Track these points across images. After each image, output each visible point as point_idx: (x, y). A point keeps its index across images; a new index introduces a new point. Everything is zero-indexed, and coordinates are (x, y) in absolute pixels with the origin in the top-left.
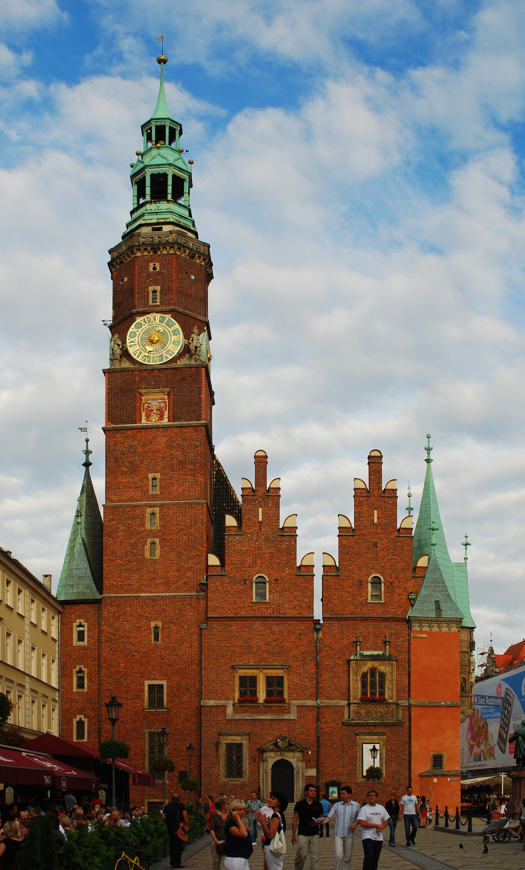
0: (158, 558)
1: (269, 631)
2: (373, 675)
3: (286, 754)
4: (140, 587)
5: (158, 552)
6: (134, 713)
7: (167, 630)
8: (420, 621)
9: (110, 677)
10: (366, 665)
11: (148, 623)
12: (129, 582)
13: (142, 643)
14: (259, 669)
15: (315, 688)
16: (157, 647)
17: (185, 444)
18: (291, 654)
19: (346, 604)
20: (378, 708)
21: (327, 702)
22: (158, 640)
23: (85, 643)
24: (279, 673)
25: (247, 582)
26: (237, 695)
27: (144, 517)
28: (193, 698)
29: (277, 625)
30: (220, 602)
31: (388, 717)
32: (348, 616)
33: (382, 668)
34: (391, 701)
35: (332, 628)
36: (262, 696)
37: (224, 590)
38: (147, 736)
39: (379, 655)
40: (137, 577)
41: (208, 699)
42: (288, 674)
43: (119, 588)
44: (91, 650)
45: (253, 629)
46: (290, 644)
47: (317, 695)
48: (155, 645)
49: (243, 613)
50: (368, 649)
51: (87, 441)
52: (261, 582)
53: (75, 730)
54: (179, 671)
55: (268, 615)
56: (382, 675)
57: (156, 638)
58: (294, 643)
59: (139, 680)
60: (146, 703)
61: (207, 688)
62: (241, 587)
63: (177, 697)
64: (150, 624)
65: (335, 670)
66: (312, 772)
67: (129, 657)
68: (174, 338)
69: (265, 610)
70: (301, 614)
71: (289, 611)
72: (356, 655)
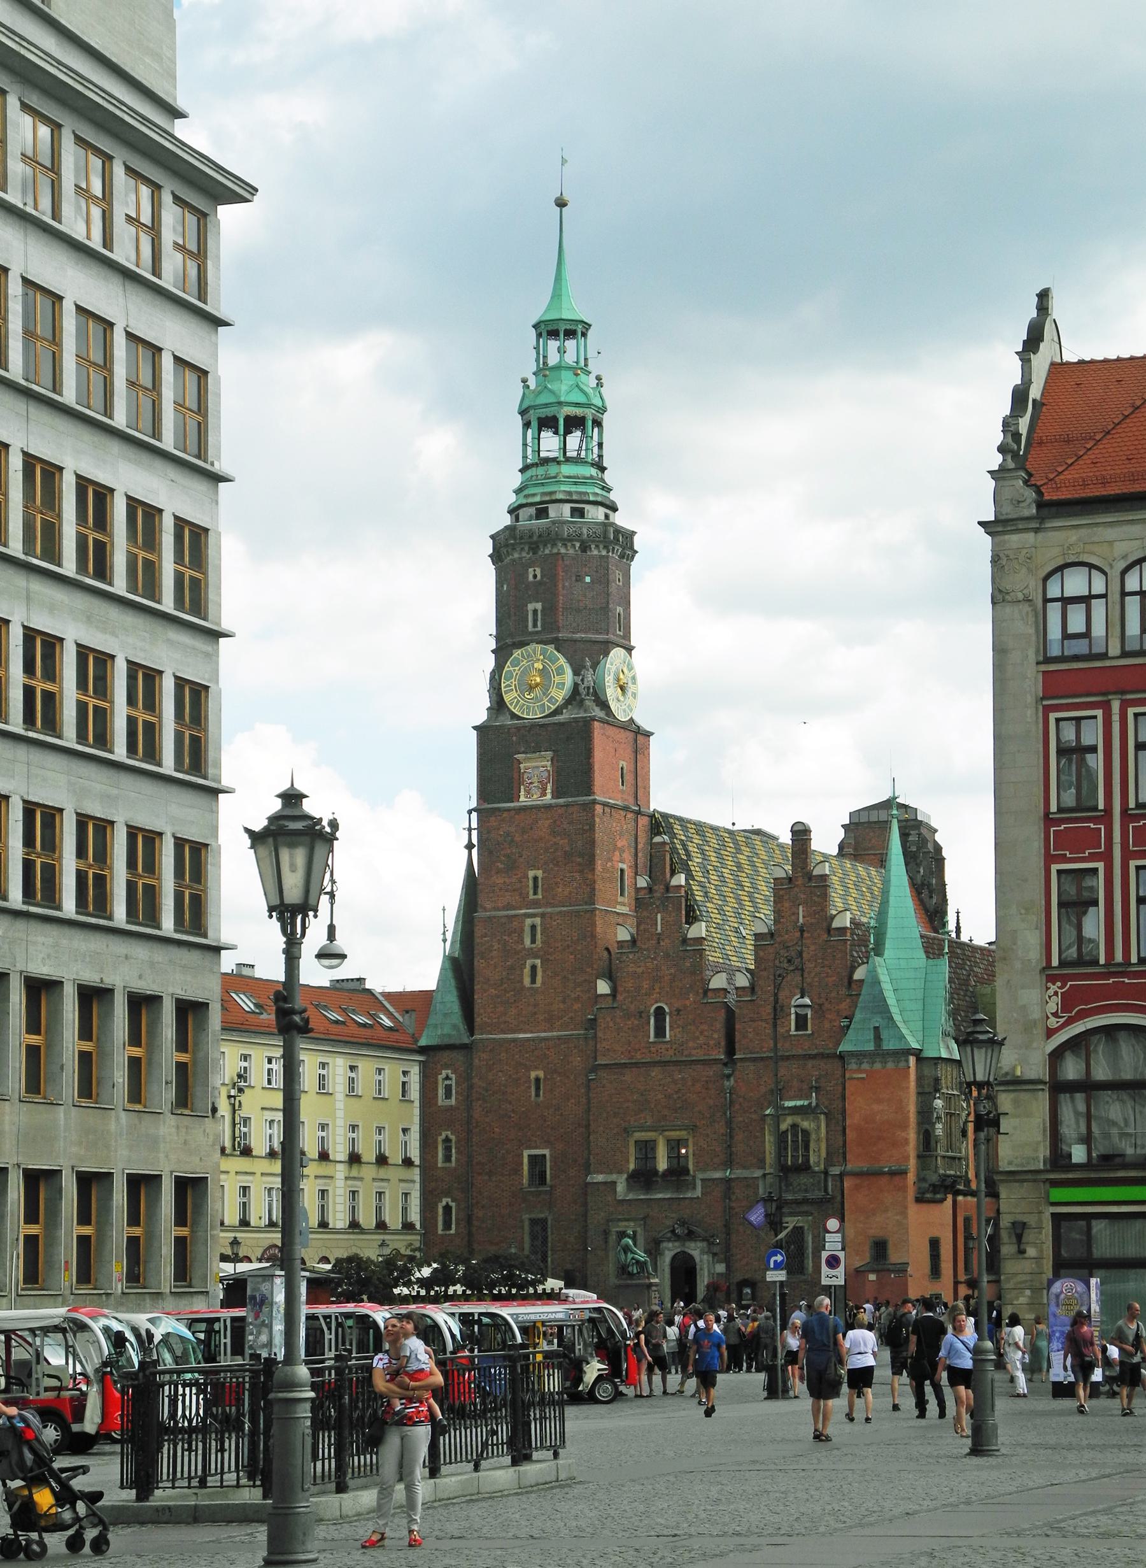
1: (669, 1079)
2: (795, 1135)
3: (687, 1244)
5: (539, 979)
10: (785, 1120)
21: (739, 1173)
23: (453, 1101)
24: (682, 1134)
27: (522, 931)
29: (680, 1072)
33: (805, 1124)
38: (527, 1223)
39: (803, 1106)
47: (729, 1163)
50: (791, 1099)
52: (660, 1013)
53: (440, 1219)
55: (668, 1059)
56: (806, 1133)
57: (537, 1095)
60: (525, 1181)
62: (636, 1022)
66: (721, 1268)
68: (557, 679)
71: (694, 1052)
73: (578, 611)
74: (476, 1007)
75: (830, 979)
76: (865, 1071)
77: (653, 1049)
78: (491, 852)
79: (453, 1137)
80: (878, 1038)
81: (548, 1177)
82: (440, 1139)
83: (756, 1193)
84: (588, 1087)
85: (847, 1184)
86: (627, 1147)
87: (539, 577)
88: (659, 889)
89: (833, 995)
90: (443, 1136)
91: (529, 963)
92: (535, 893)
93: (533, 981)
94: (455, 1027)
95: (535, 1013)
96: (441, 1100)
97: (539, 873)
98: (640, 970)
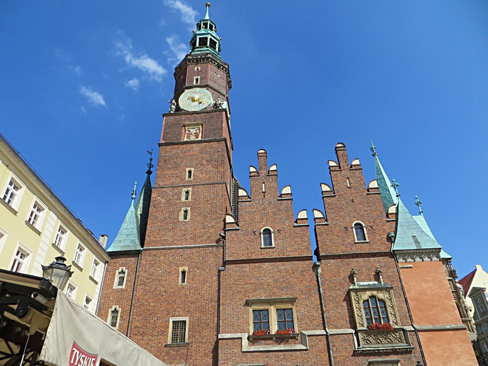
0: (189, 220)
5: (189, 217)
6: (157, 349)
7: (192, 273)
9: (140, 315)
11: (177, 268)
19: (338, 245)
22: (184, 282)
25: (256, 233)
27: (181, 193)
28: (212, 333)
30: (235, 248)
33: (380, 295)
34: (396, 327)
35: (329, 265)
36: (274, 329)
37: (239, 240)
41: (226, 332)
43: (157, 243)
45: (262, 269)
48: (182, 285)
49: (254, 257)
50: (363, 280)
51: (151, 160)
54: (200, 307)
56: (382, 301)
57: (183, 281)
58: (298, 279)
59: (165, 317)
62: (252, 237)
63: (198, 332)
64: (179, 269)
65: (338, 300)
70: (301, 255)
78: (165, 161)
79: (120, 310)
80: (417, 242)
82: (110, 311)
84: (219, 276)
88: (263, 173)
89: (378, 221)
90: (113, 309)
91: (183, 209)
93: (185, 218)
94: (133, 241)
95: (185, 235)
96: (115, 286)
98: (254, 210)
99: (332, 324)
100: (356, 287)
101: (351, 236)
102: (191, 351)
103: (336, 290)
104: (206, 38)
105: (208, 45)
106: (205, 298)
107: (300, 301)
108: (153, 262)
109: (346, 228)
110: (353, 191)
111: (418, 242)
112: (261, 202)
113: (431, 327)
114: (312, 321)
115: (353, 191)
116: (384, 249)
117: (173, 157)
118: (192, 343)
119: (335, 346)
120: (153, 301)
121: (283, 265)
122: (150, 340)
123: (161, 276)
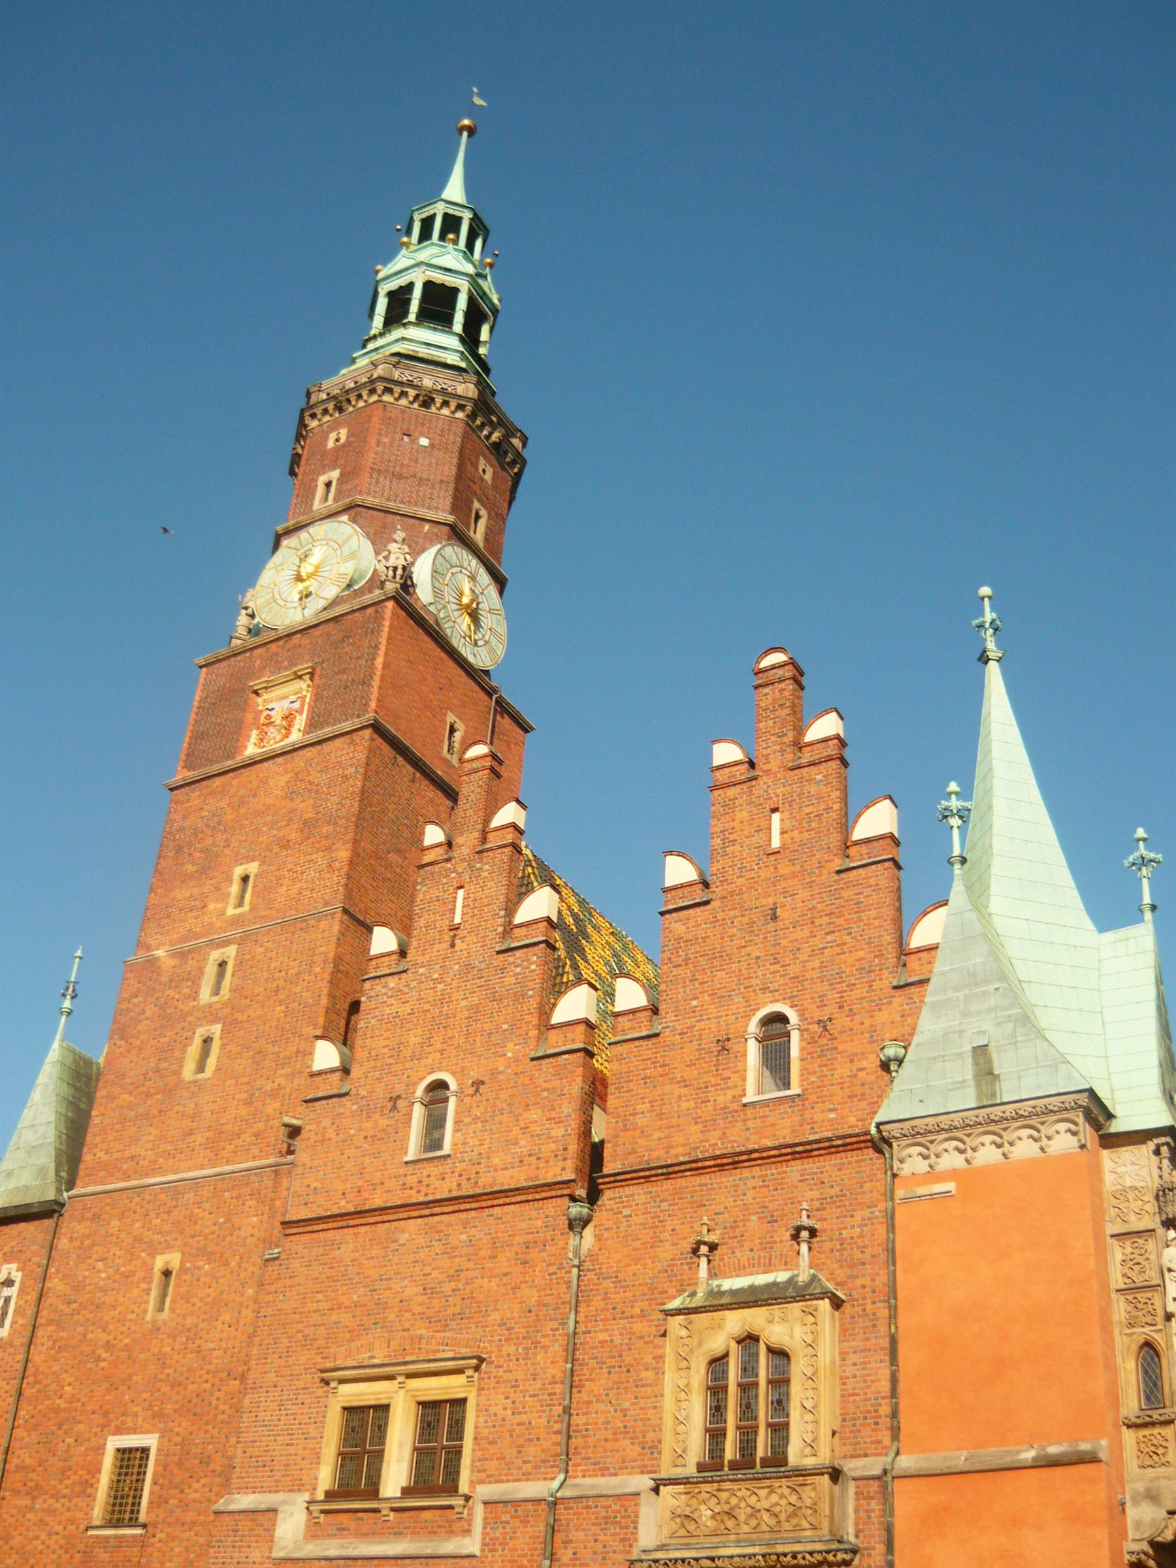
1: (438, 1247)
2: (749, 1369)
4: (155, 1162)
5: (212, 1062)
6: (63, 1542)
7: (188, 1276)
8: (925, 1133)
9: (36, 1427)
12: (135, 1150)
13: (125, 1320)
14: (391, 1377)
15: (559, 1432)
16: (156, 1328)
17: (324, 778)
18: (496, 1316)
19: (674, 1121)
20: (763, 1493)
26: (325, 1477)
31: (798, 1528)
32: (682, 1159)
34: (810, 1462)
35: (626, 1212)
36: (396, 1474)
37: (342, 1137)
40: (154, 1132)
42: (480, 1389)
44: (12, 1350)
45: (395, 1246)
46: (494, 1284)
47: (566, 1457)
48: (154, 1323)
54: (195, 1400)
58: (505, 1279)
60: (98, 1512)
61: (250, 1451)
62: (383, 1122)
63: (176, 1487)
65: (628, 1359)
67: (89, 1365)
69: (437, 1183)
72: (693, 1294)
73: (401, 477)
74: (92, 1130)
75: (849, 958)
76: (953, 1175)
77: (411, 1180)
78: (179, 849)
81: (145, 1502)
83: (629, 1540)
85: (906, 1499)
86: (321, 1423)
87: (343, 440)
88: (467, 842)
91: (200, 1033)
92: (240, 903)
93: (201, 1068)
94: (42, 1171)
95: (191, 1133)
97: (253, 868)
99: (589, 1458)
100: (699, 1299)
101: (734, 1077)
102: (149, 1550)
103: (632, 1317)
104: (411, 286)
105: (412, 317)
106: (212, 1367)
107: (497, 1367)
108: (87, 1242)
109: (725, 1046)
110: (785, 869)
111: (991, 1073)
112: (435, 972)
113: (960, 1459)
114: (522, 1446)
115: (785, 869)
116: (852, 1123)
117: (202, 832)
118: (155, 1525)
119: (571, 1542)
120: (71, 1379)
121: (465, 1224)
122: (49, 1511)
123: (102, 1290)
